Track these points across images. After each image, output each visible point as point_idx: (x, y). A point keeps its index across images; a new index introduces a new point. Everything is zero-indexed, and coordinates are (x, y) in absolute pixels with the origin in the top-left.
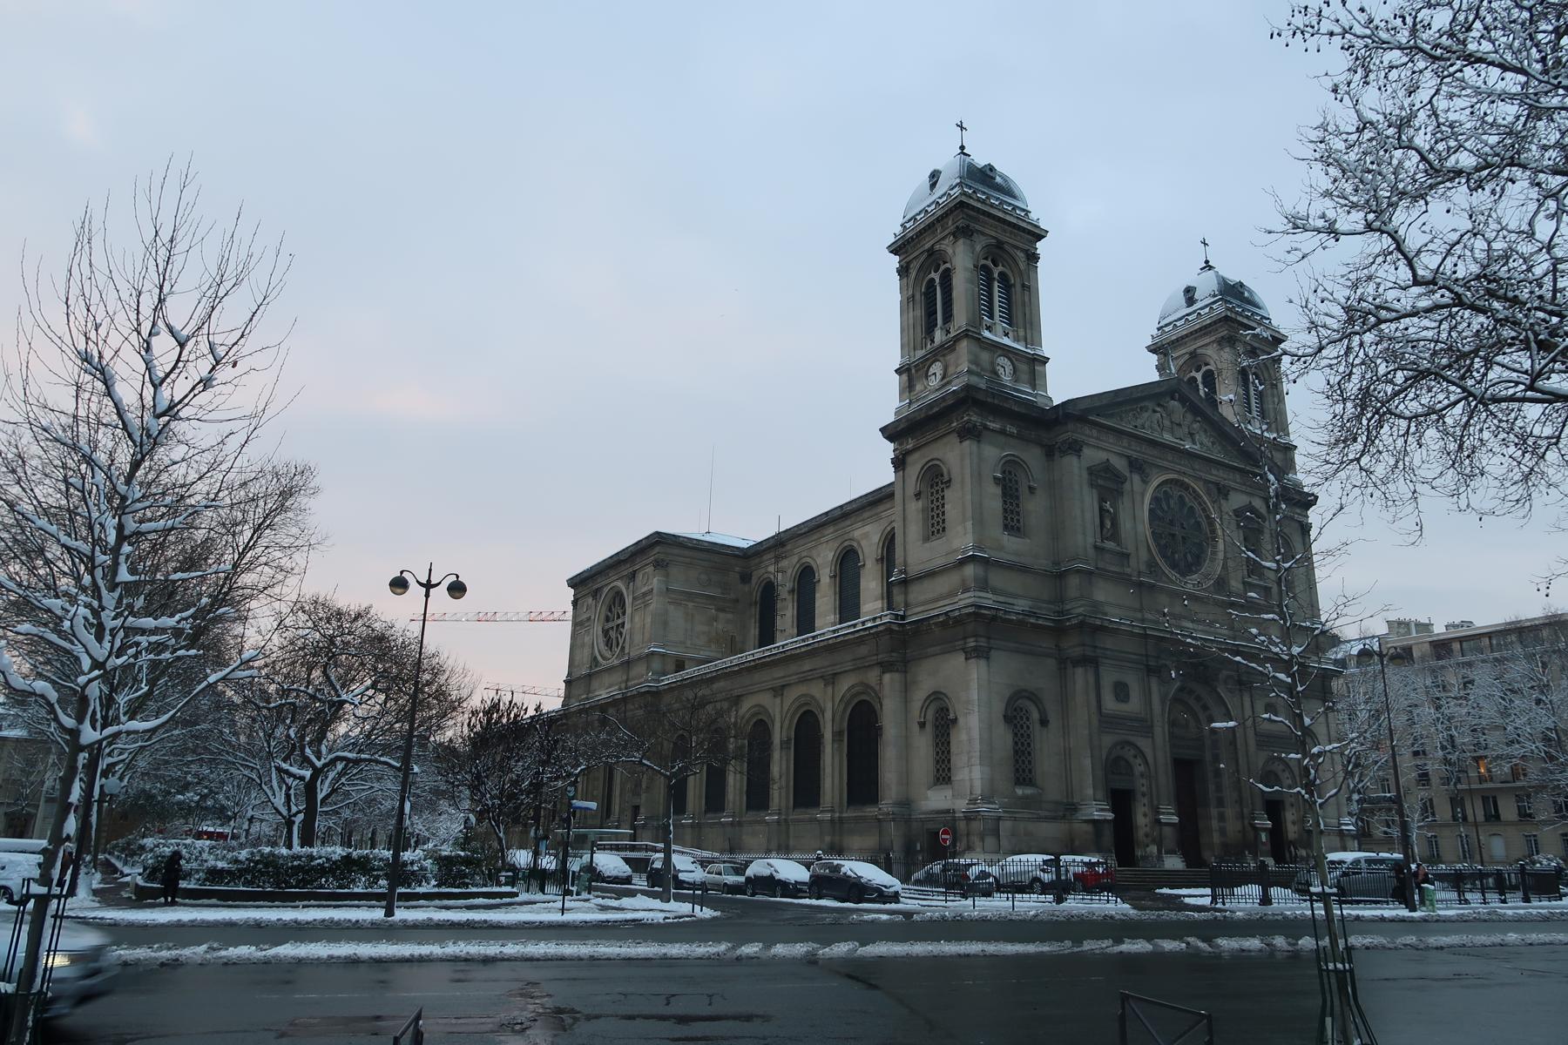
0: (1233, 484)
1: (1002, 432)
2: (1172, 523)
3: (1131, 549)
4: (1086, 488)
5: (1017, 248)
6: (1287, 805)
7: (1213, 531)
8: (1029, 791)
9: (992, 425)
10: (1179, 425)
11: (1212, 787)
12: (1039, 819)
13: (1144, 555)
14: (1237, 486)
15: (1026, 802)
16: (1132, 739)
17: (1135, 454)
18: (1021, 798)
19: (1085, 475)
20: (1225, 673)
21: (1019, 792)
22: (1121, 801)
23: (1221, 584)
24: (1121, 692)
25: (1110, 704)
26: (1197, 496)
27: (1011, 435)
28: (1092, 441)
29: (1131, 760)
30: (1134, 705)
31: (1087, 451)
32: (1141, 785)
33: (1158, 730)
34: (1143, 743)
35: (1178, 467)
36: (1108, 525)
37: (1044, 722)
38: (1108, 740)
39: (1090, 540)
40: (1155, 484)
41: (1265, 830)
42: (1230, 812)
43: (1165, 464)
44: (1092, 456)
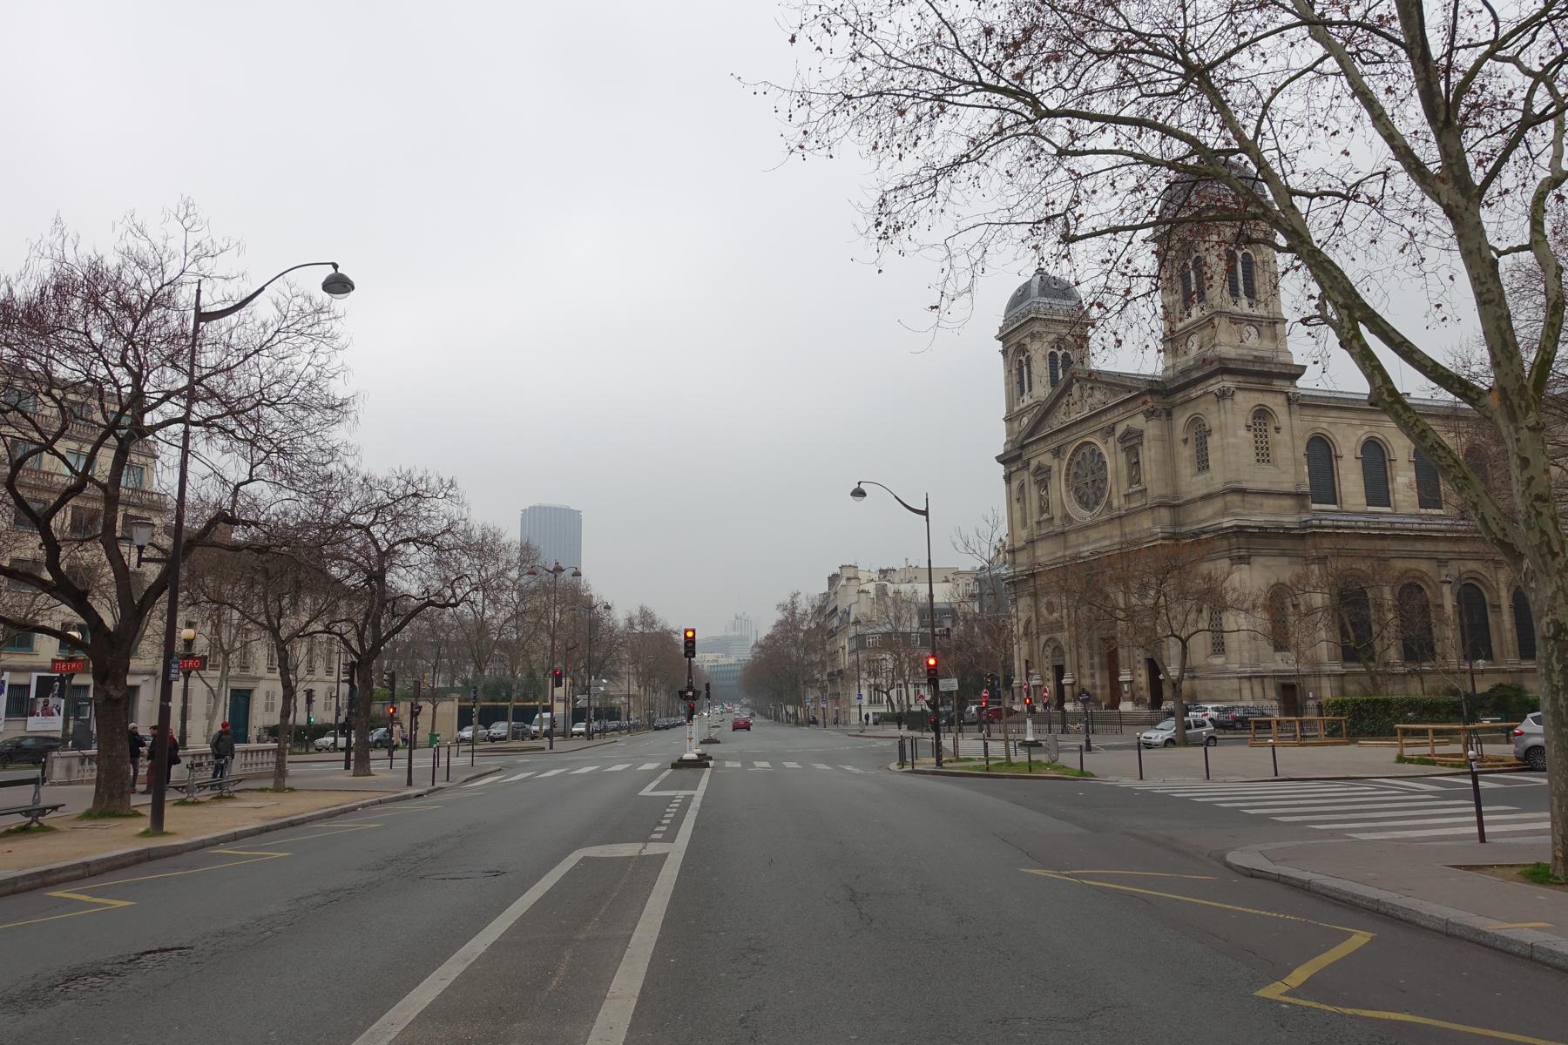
23: (1109, 504)
24: (1051, 608)
34: (1058, 635)
44: (1034, 463)
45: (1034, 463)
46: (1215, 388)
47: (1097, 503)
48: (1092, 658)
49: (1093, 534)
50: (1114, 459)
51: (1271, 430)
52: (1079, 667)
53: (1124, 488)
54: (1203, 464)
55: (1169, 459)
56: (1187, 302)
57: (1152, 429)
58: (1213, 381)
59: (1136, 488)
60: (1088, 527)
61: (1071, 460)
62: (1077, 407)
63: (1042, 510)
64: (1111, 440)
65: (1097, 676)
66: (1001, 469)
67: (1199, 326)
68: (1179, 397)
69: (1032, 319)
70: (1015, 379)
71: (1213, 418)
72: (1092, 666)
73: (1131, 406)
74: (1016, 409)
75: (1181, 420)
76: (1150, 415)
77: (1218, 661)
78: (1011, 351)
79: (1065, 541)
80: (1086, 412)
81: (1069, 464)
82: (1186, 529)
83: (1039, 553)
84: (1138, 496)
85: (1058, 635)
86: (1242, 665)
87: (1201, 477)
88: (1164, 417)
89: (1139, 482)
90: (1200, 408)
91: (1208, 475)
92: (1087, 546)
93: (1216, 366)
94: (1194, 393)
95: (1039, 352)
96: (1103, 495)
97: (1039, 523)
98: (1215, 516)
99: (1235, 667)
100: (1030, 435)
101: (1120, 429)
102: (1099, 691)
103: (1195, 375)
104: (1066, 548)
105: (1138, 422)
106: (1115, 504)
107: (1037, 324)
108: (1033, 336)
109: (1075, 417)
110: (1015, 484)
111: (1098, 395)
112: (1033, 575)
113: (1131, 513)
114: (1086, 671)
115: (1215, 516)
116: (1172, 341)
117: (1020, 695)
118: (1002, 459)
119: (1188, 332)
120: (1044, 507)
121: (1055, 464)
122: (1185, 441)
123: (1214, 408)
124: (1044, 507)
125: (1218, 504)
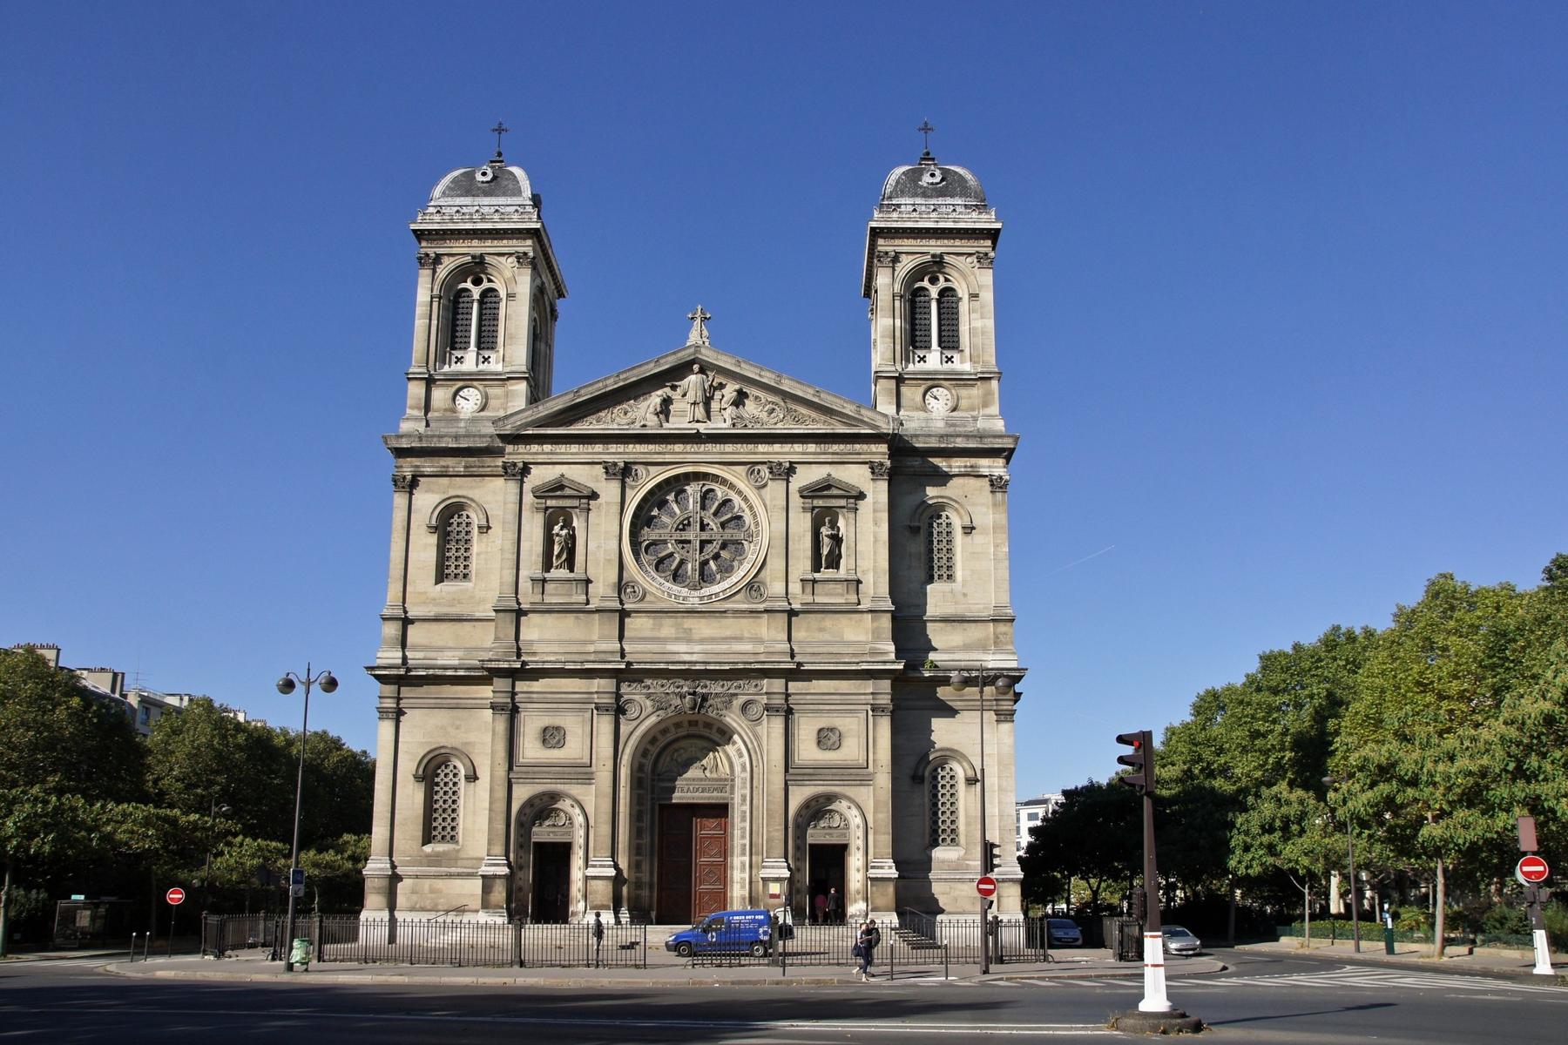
0: (795, 458)
6: (853, 848)
7: (757, 524)
11: (737, 833)
12: (450, 876)
15: (435, 860)
16: (560, 787)
18: (428, 856)
19: (528, 498)
20: (742, 699)
21: (428, 849)
23: (753, 586)
24: (552, 736)
26: (732, 486)
29: (569, 810)
30: (574, 748)
31: (535, 471)
32: (579, 840)
35: (690, 458)
36: (561, 550)
37: (472, 777)
42: (747, 859)
43: (668, 458)
44: (540, 476)
49: (703, 627)
50: (772, 518)
53: (802, 564)
65: (645, 867)
81: (645, 499)
84: (840, 588)
85: (575, 790)
92: (693, 645)
96: (727, 570)
98: (967, 648)
102: (645, 893)
103: (960, 443)
105: (855, 476)
106: (777, 588)
109: (679, 422)
112: (514, 675)
115: (967, 648)
119: (932, 381)
121: (609, 491)
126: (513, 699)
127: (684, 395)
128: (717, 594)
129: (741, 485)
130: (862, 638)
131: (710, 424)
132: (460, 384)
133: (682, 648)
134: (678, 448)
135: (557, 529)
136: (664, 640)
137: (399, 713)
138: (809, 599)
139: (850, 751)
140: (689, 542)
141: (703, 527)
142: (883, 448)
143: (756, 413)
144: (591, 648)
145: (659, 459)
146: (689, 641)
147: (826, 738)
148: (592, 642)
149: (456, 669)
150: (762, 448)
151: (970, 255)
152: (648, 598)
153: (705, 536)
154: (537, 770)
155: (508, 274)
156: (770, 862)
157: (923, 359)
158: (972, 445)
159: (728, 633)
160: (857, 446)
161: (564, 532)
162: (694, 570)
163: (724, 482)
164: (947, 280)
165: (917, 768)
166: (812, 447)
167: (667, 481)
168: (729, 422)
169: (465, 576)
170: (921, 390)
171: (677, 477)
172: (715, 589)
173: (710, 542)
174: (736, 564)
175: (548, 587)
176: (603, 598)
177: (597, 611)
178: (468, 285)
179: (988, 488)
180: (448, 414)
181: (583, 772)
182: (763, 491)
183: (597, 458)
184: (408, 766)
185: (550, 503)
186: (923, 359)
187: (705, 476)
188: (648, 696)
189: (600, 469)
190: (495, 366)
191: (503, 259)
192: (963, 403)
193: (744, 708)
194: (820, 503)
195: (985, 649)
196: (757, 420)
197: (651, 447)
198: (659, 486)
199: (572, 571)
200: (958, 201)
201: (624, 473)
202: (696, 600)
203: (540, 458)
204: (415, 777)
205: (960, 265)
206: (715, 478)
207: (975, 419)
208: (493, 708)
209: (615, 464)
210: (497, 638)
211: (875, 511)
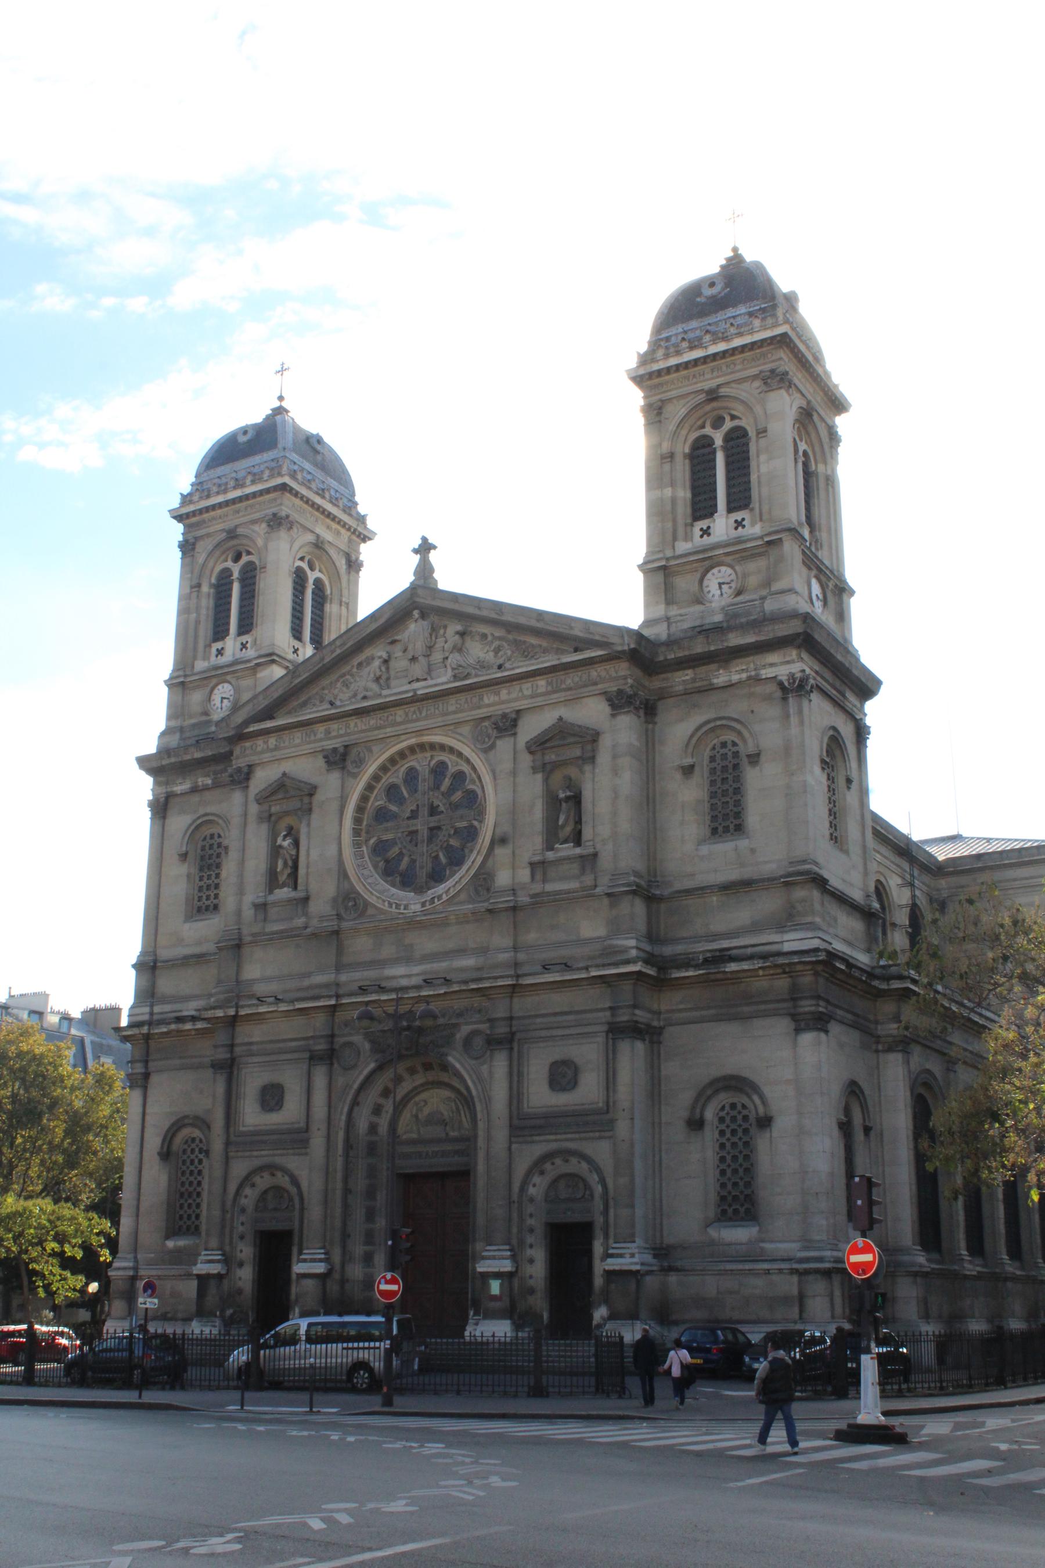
1: (194, 790)
2: (414, 815)
3: (314, 887)
4: (252, 826)
5: (254, 522)
8: (182, 1242)
9: (178, 789)
10: (414, 659)
13: (330, 889)
14: (539, 701)
16: (277, 1160)
17: (329, 744)
19: (254, 808)
20: (465, 1029)
21: (170, 1244)
22: (275, 1249)
23: (483, 880)
24: (272, 1097)
25: (252, 1116)
26: (460, 755)
27: (206, 788)
28: (266, 757)
30: (291, 1112)
33: (317, 1141)
34: (293, 1163)
38: (239, 1169)
39: (249, 898)
40: (372, 768)
41: (497, 1275)
45: (263, 778)
46: (782, 672)
47: (437, 876)
48: (370, 1215)
49: (426, 943)
51: (841, 782)
52: (345, 1236)
53: (531, 845)
54: (726, 817)
55: (649, 801)
56: (702, 506)
57: (622, 732)
58: (773, 658)
59: (567, 850)
60: (413, 924)
61: (376, 778)
62: (418, 670)
63: (272, 881)
64: (504, 746)
66: (144, 786)
67: (739, 553)
68: (682, 678)
69: (284, 487)
70: (207, 603)
71: (766, 729)
72: (369, 1238)
73: (572, 679)
74: (200, 665)
75: (678, 730)
76: (618, 702)
77: (739, 1234)
78: (203, 549)
79: (340, 951)
80: (443, 680)
81: (369, 788)
82: (680, 948)
83: (252, 971)
85: (293, 1163)
86: (807, 1243)
87: (725, 848)
88: (642, 713)
89: (577, 838)
90: (736, 708)
91: (743, 843)
93: (794, 627)
94: (721, 678)
95: (281, 557)
96: (457, 860)
97: (262, 907)
98: (755, 928)
99: (790, 1248)
100: (269, 713)
101: (531, 727)
103: (735, 640)
104: (339, 968)
105: (592, 712)
106: (503, 878)
107: (288, 499)
108: (277, 522)
109: (400, 688)
110: (179, 823)
111: (477, 651)
112: (233, 1021)
113: (539, 900)
114: (358, 1249)
115: (755, 928)
116: (662, 573)
117: (130, 1297)
118: (145, 763)
120: (285, 870)
121: (330, 783)
122: (688, 771)
123: (773, 711)
124: (285, 870)
125: (769, 903)
126: (232, 1052)
127: (405, 651)
128: (439, 897)
129: (467, 751)
130: (602, 932)
131: (430, 682)
132: (214, 681)
133: (399, 970)
134: (399, 714)
135: (279, 841)
136: (382, 963)
137: (146, 1076)
138: (537, 888)
139: (589, 1090)
140: (417, 831)
141: (433, 811)
142: (623, 668)
143: (482, 655)
144: (306, 982)
145: (380, 734)
146: (408, 960)
147: (563, 1075)
148: (309, 975)
149: (193, 1019)
150: (489, 698)
151: (755, 377)
152: (370, 911)
153: (433, 821)
154: (257, 1139)
155: (260, 542)
156: (491, 1250)
157: (706, 532)
158: (750, 639)
159: (451, 945)
160: (594, 674)
161: (286, 844)
162: (422, 867)
163: (452, 750)
164: (733, 417)
165: (693, 1108)
166: (542, 683)
167: (392, 761)
168: (450, 673)
169: (216, 907)
170: (698, 575)
171: (402, 754)
172: (441, 889)
173: (439, 828)
174: (466, 851)
175: (273, 912)
176: (322, 918)
177: (314, 935)
178: (229, 564)
179: (779, 694)
180: (204, 718)
181: (297, 1138)
182: (491, 754)
183: (318, 746)
184: (154, 1143)
185: (273, 810)
186: (706, 532)
187: (432, 746)
188: (367, 1036)
189: (320, 762)
190: (250, 653)
191: (256, 527)
192: (753, 581)
193: (467, 1042)
194: (551, 757)
195: (781, 927)
196: (482, 665)
197: (372, 722)
198: (384, 768)
199: (295, 888)
200: (742, 309)
201: (340, 759)
202: (418, 907)
203: (266, 757)
204: (159, 1154)
205: (743, 396)
206: (442, 747)
207: (763, 598)
208: (213, 1066)
209: (335, 750)
210: (219, 982)
211: (615, 757)
